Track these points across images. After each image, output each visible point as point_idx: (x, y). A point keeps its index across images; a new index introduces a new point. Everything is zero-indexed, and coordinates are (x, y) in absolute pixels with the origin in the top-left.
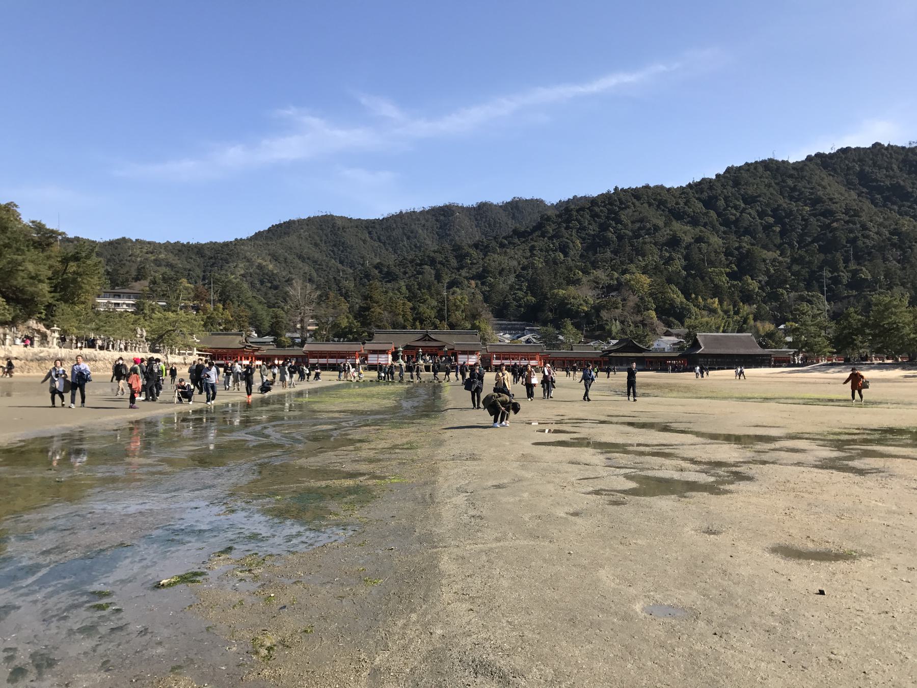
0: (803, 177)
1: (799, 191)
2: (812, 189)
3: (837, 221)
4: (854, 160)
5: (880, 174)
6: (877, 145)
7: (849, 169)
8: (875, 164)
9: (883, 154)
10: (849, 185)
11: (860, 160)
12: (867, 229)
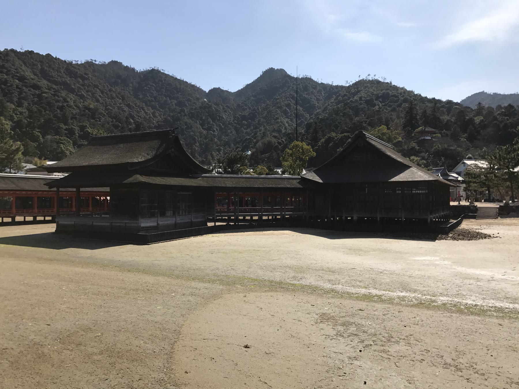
0: (8, 61)
1: (6, 68)
2: (16, 70)
3: (46, 93)
4: (36, 61)
5: (54, 74)
6: (48, 55)
7: (34, 65)
8: (50, 66)
9: (54, 62)
10: (35, 74)
11: (41, 62)
12: (68, 102)
